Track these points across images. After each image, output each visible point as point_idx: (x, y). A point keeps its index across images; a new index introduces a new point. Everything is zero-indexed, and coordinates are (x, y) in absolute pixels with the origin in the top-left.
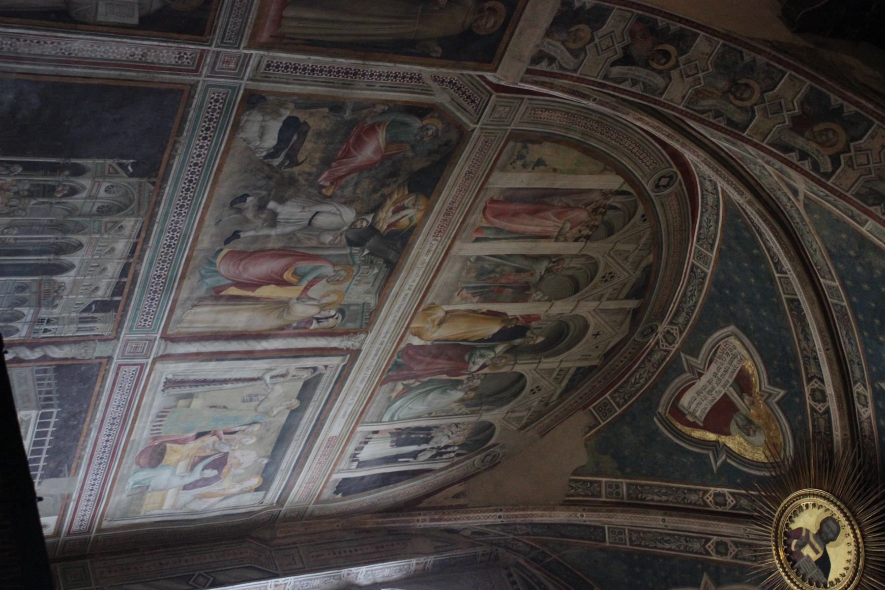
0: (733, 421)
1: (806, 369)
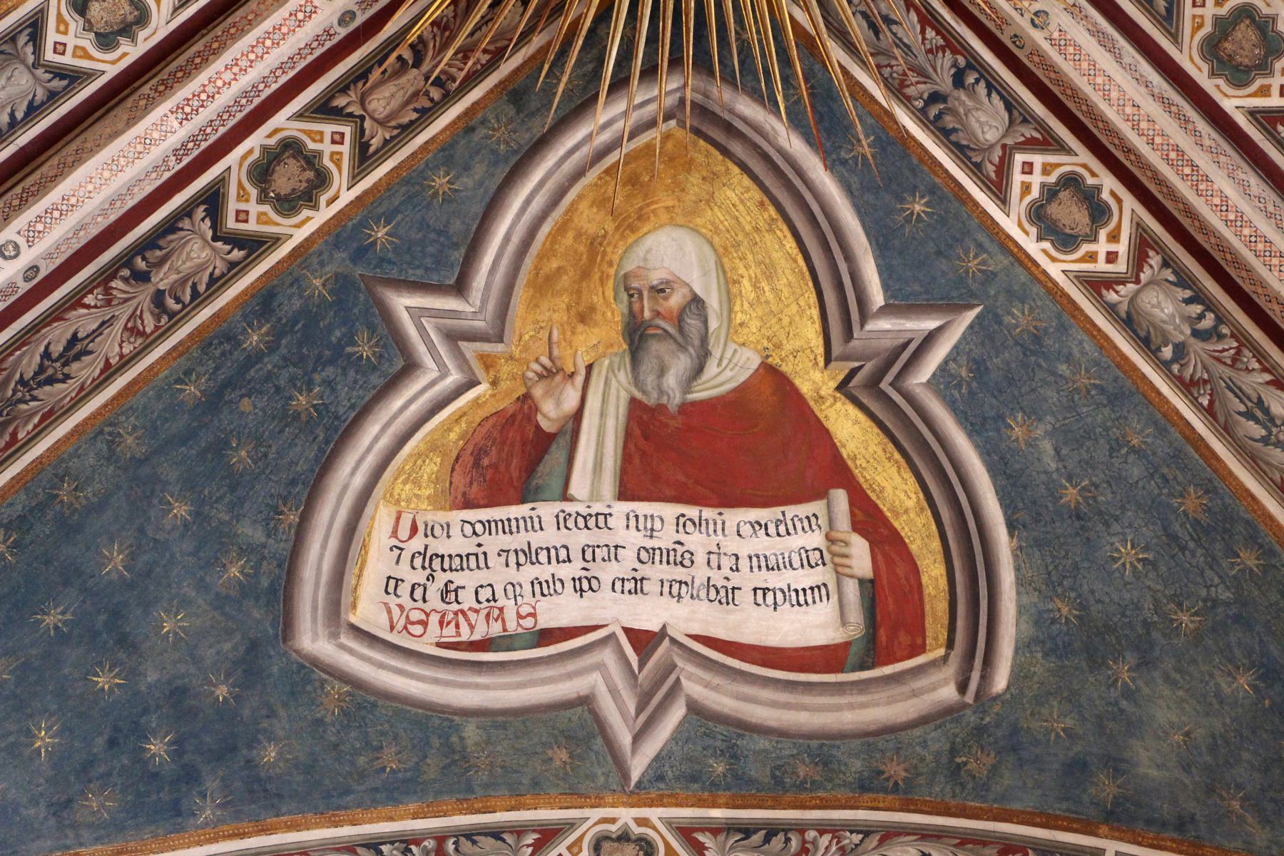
0: (700, 394)
1: (217, 283)
